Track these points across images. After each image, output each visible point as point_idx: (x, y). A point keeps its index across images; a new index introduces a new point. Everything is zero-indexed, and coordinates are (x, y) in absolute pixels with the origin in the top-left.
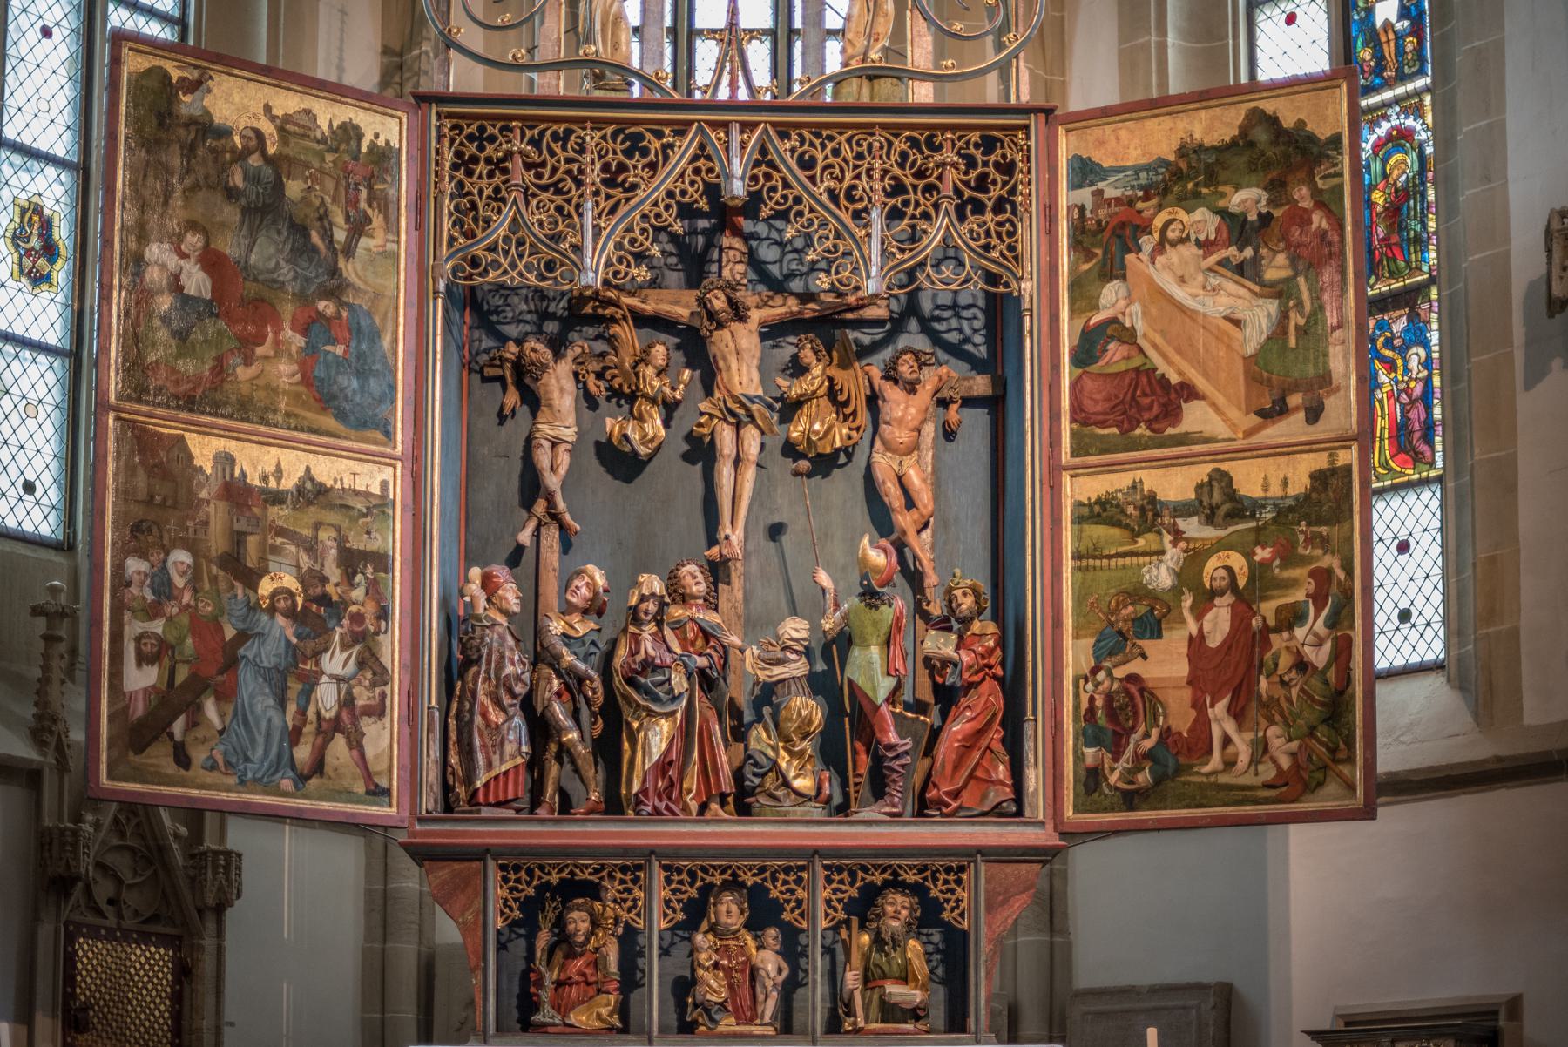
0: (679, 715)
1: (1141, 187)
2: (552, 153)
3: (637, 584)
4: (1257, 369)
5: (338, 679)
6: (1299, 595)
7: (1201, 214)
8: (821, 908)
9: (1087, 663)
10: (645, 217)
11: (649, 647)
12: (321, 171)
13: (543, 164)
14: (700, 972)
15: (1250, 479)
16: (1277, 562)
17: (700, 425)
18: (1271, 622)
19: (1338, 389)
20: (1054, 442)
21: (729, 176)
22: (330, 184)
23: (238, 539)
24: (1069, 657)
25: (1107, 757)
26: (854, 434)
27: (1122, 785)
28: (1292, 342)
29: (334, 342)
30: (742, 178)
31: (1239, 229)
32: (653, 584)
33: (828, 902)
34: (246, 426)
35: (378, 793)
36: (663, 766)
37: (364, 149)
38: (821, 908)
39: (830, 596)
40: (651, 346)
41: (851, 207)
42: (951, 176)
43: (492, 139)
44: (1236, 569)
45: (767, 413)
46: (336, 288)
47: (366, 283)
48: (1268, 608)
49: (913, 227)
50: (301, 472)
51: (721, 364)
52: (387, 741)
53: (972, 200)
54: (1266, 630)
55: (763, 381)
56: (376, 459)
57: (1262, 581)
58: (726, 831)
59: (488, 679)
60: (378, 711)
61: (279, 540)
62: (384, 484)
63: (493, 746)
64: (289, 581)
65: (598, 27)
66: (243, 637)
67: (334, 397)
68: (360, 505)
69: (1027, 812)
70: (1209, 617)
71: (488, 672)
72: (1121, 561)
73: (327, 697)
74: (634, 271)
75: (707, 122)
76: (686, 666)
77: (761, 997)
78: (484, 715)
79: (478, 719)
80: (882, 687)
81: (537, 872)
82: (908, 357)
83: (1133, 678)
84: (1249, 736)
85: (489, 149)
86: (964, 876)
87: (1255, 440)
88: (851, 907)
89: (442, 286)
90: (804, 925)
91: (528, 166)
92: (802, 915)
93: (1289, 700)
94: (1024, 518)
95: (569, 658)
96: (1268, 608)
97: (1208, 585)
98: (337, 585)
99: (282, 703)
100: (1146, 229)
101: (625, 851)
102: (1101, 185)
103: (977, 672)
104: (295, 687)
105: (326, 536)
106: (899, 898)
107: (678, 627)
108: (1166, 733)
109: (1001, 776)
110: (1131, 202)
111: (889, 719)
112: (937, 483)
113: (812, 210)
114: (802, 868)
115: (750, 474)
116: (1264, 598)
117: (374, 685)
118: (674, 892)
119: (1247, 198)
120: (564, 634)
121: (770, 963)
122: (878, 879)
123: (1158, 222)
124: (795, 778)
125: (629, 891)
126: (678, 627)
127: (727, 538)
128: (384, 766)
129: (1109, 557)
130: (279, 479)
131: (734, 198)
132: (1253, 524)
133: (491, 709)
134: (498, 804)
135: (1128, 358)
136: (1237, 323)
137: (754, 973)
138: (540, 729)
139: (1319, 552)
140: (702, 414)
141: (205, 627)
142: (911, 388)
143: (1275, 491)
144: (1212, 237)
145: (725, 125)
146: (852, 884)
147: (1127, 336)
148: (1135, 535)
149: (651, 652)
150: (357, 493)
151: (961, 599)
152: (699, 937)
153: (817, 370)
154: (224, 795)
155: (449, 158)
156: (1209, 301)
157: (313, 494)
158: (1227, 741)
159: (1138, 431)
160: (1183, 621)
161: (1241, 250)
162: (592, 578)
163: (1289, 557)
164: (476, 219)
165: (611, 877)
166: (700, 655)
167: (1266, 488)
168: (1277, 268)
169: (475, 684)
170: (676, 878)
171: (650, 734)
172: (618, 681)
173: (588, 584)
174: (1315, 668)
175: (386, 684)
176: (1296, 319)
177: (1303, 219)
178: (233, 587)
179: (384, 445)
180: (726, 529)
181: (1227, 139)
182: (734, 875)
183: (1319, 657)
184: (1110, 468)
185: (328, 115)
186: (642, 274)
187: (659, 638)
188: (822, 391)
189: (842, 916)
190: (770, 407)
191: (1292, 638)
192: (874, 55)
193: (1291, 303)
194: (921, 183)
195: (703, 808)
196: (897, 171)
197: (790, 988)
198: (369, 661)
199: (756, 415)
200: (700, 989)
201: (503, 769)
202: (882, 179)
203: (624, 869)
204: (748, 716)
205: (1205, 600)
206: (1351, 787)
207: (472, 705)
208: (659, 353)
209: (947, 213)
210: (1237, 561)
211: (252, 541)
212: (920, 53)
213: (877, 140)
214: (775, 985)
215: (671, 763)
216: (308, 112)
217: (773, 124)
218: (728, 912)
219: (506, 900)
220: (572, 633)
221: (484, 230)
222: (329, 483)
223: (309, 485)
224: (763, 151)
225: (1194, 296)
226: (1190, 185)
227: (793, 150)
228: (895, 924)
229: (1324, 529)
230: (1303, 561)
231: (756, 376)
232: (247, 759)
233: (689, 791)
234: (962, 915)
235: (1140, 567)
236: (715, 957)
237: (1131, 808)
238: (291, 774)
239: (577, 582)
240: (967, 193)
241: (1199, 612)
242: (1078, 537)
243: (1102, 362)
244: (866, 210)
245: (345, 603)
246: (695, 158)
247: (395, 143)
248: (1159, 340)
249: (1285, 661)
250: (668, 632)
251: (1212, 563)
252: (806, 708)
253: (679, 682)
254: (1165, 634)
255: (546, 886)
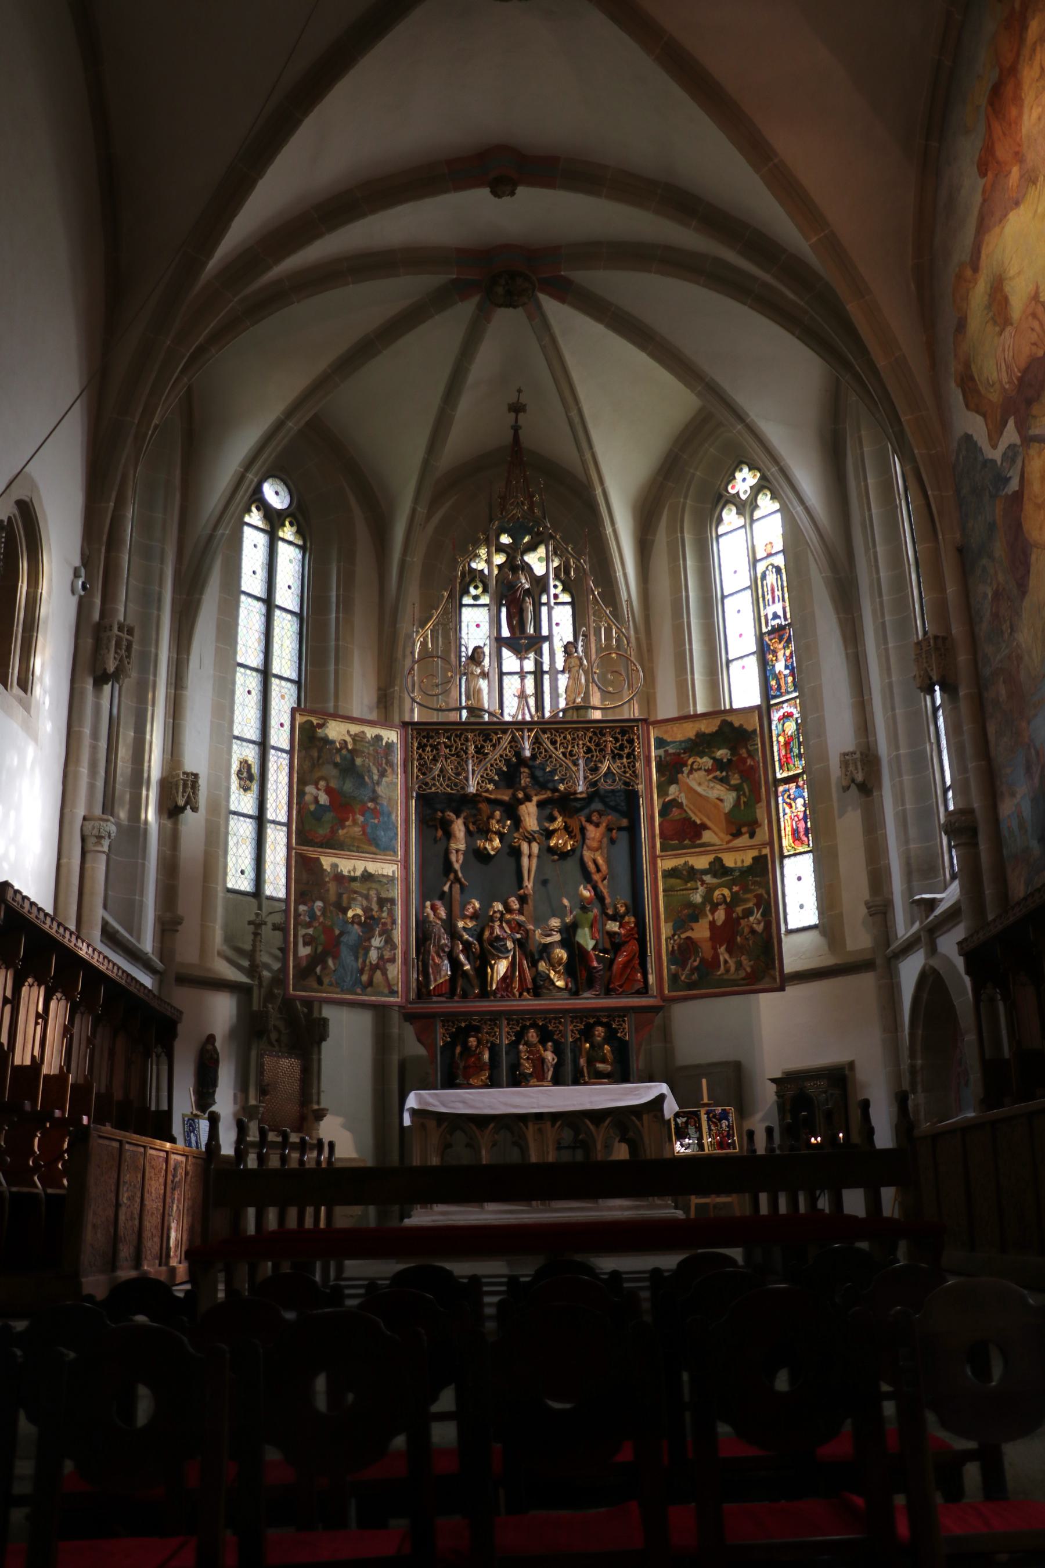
0: (510, 958)
1: (682, 749)
2: (455, 742)
3: (492, 907)
4: (730, 817)
5: (378, 948)
6: (750, 905)
7: (705, 759)
8: (569, 1034)
9: (670, 933)
10: (492, 765)
11: (497, 931)
12: (368, 754)
13: (452, 746)
14: (522, 1061)
15: (730, 860)
16: (741, 892)
17: (515, 842)
18: (740, 915)
19: (760, 825)
20: (653, 846)
21: (524, 749)
22: (372, 758)
23: (340, 896)
24: (663, 930)
25: (680, 970)
26: (575, 843)
27: (686, 980)
28: (742, 807)
29: (374, 819)
30: (529, 749)
31: (719, 764)
32: (499, 906)
33: (572, 1031)
34: (342, 852)
35: (393, 993)
36: (505, 977)
37: (384, 744)
38: (569, 1034)
39: (568, 909)
40: (495, 811)
41: (571, 758)
42: (609, 745)
43: (432, 737)
44: (726, 894)
45: (541, 837)
46: (375, 798)
47: (385, 794)
48: (739, 910)
49: (596, 765)
50: (363, 869)
51: (522, 818)
52: (396, 972)
53: (618, 754)
54: (738, 918)
55: (540, 824)
56: (390, 862)
57: (736, 899)
58: (530, 1003)
60: (393, 960)
61: (355, 895)
62: (393, 872)
64: (359, 911)
65: (472, 693)
66: (342, 934)
67: (374, 839)
68: (385, 880)
69: (650, 992)
70: (716, 913)
71: (434, 943)
72: (682, 892)
73: (373, 955)
74: (488, 786)
75: (515, 729)
76: (512, 938)
77: (546, 1070)
78: (433, 960)
79: (431, 962)
80: (590, 944)
81: (456, 1022)
82: (595, 814)
83: (688, 938)
84: (734, 960)
85: (431, 741)
86: (626, 1019)
87: (731, 845)
88: (581, 1032)
89: (414, 795)
90: (563, 1040)
91: (446, 747)
92: (562, 1036)
93: (749, 945)
94: (643, 876)
95: (466, 936)
96: (739, 910)
97: (715, 901)
98: (377, 912)
99: (357, 959)
100: (686, 765)
101: (491, 1013)
102: (667, 748)
103: (627, 937)
104: (361, 952)
105: (373, 893)
106: (600, 1028)
107: (508, 922)
108: (702, 960)
109: (639, 978)
110: (679, 754)
111: (594, 957)
112: (608, 861)
113: (556, 760)
114: (561, 1018)
115: (535, 861)
116: (739, 906)
117: (391, 950)
118: (511, 1028)
119: (722, 753)
120: (464, 927)
121: (549, 1056)
122: (591, 1021)
123: (690, 761)
124: (557, 981)
125: (493, 1029)
126: (508, 922)
127: (527, 886)
128: (395, 982)
129: (677, 891)
130: (354, 872)
131: (526, 757)
132: (731, 877)
133: (436, 958)
134: (439, 996)
135: (680, 814)
136: (721, 800)
137: (542, 1060)
138: (455, 964)
139: (757, 887)
140: (515, 838)
141: (328, 930)
142: (597, 825)
143: (739, 864)
144: (710, 768)
145: (522, 730)
146: (581, 1024)
147: (680, 805)
148: (687, 882)
149: (499, 933)
150: (383, 876)
151: (620, 908)
152: (521, 1047)
153: (560, 819)
154: (335, 996)
155: (416, 745)
156: (710, 792)
157: (367, 877)
158: (726, 962)
159: (686, 842)
160: (706, 915)
161: (721, 773)
162: (474, 904)
163: (745, 889)
164: (427, 768)
165: (485, 1023)
166: (518, 933)
167: (736, 863)
168: (735, 780)
170: (511, 1023)
171: (499, 966)
172: (486, 945)
173: (473, 907)
174: (758, 932)
175: (395, 949)
176: (743, 799)
177: (744, 761)
178: (338, 914)
179: (393, 856)
180: (526, 883)
181: (714, 731)
182: (534, 1021)
183: (759, 928)
184: (676, 856)
185: (370, 732)
186: (491, 787)
187: (501, 927)
188: (562, 827)
189: (578, 1036)
190: (542, 834)
191: (749, 921)
192: (579, 700)
193: (741, 793)
194: (598, 748)
195: (521, 995)
196: (588, 744)
197: (557, 1067)
198: (389, 941)
199: (537, 838)
200: (522, 1068)
202: (583, 748)
203: (490, 1020)
204: (537, 957)
205: (714, 908)
206: (775, 979)
207: (429, 956)
208: (498, 813)
209: (608, 760)
210: (726, 892)
211: (345, 896)
212: (596, 699)
213: (581, 733)
214: (552, 1065)
216: (363, 732)
217: (540, 729)
218: (532, 1036)
219: (444, 1034)
220: (467, 926)
221: (430, 772)
222: (373, 872)
223: (366, 874)
224: (536, 737)
225: (704, 790)
226: (701, 748)
227: (548, 738)
228: (599, 1039)
229: (758, 879)
230: (751, 891)
231: (536, 822)
232: (344, 981)
233: (515, 988)
234: (625, 1034)
235: (689, 894)
236: (527, 1055)
237: (690, 990)
238: (360, 986)
239: (469, 907)
240: (616, 751)
241: (713, 912)
242: (664, 884)
243: (671, 815)
244: (577, 759)
245: (380, 918)
246: (510, 742)
247: (395, 741)
248: (692, 807)
249: (746, 930)
250: (504, 925)
251: (717, 893)
252: (562, 954)
253: (510, 945)
254: (700, 920)
255: (459, 1028)
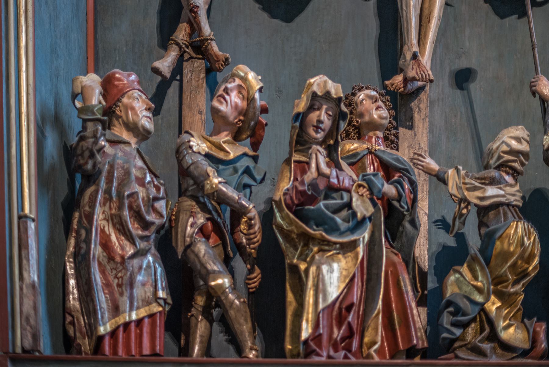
59: (108, 198)
63: (119, 286)
71: (108, 192)
78: (106, 245)
79: (96, 250)
133: (113, 238)
169: (93, 206)
201: (134, 317)
215: (349, 308)
